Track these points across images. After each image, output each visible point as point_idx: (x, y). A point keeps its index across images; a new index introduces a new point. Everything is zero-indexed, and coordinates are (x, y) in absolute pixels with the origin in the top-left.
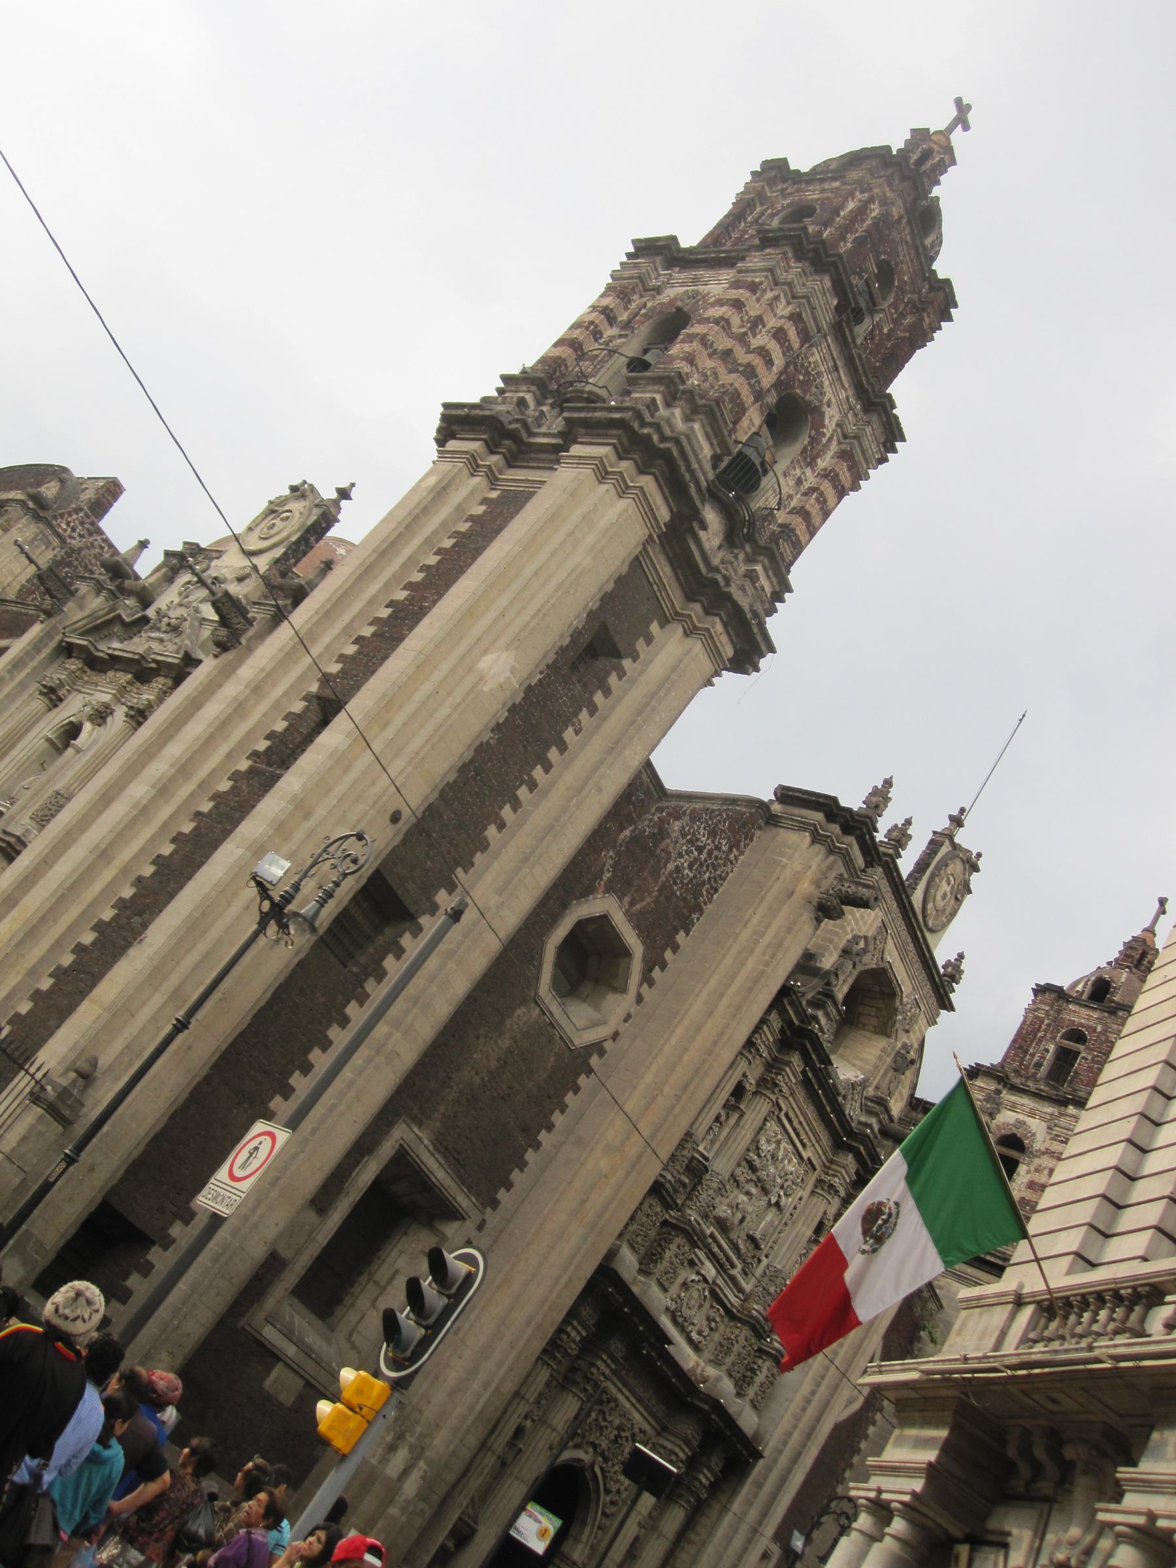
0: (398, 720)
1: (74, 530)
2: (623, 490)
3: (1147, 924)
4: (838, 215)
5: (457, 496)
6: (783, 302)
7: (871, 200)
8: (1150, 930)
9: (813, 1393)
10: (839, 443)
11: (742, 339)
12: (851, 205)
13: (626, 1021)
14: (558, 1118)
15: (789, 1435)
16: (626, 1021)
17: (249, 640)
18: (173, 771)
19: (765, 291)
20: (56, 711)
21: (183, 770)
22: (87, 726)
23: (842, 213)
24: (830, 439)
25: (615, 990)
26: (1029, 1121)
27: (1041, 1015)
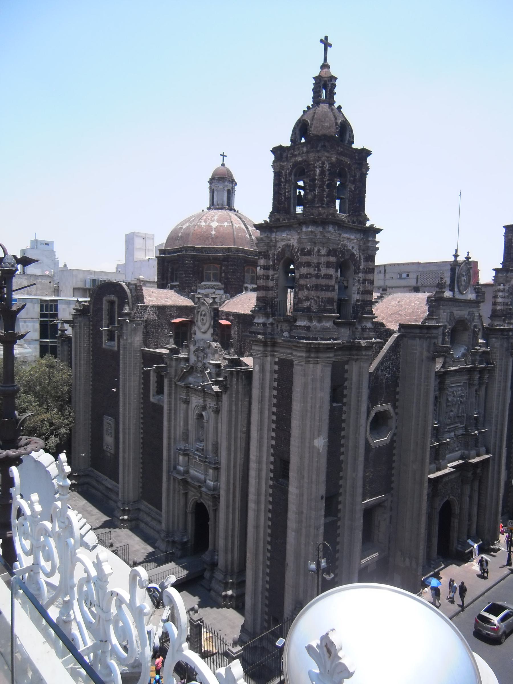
0: (306, 475)
1: (141, 313)
4: (315, 180)
5: (268, 367)
6: (321, 248)
7: (323, 163)
9: (497, 429)
10: (363, 254)
11: (317, 276)
12: (318, 171)
13: (396, 421)
14: (394, 458)
15: (495, 443)
16: (396, 421)
17: (230, 385)
18: (256, 497)
19: (314, 249)
20: (190, 405)
21: (259, 494)
22: (204, 413)
23: (316, 177)
24: (360, 257)
25: (389, 418)
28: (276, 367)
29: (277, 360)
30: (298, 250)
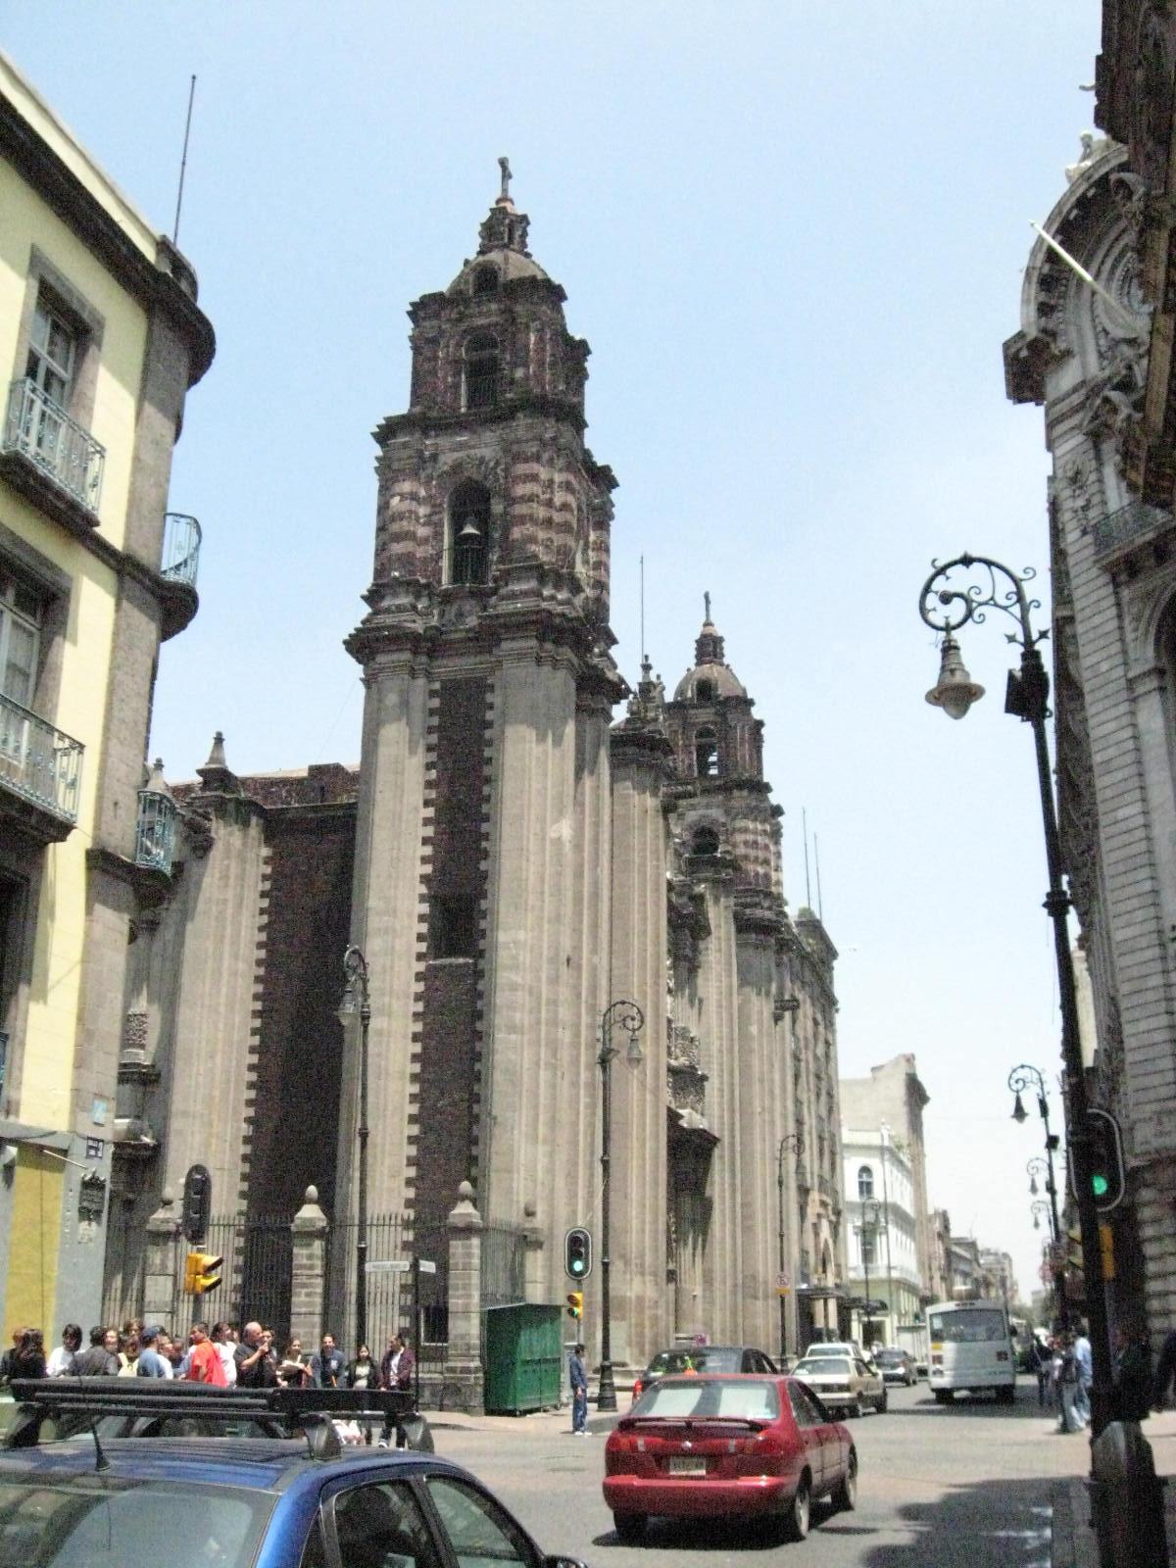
2: (555, 664)
3: (703, 620)
8: (708, 624)
9: (722, 1083)
12: (533, 338)
26: (709, 812)
27: (675, 728)
28: (436, 703)
29: (437, 686)
30: (497, 463)
